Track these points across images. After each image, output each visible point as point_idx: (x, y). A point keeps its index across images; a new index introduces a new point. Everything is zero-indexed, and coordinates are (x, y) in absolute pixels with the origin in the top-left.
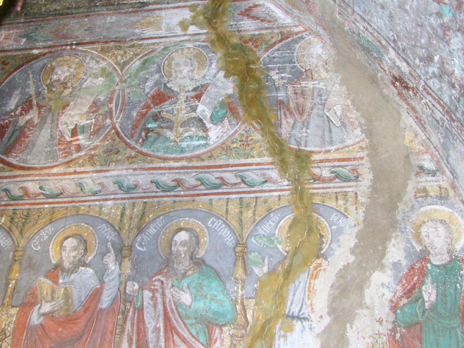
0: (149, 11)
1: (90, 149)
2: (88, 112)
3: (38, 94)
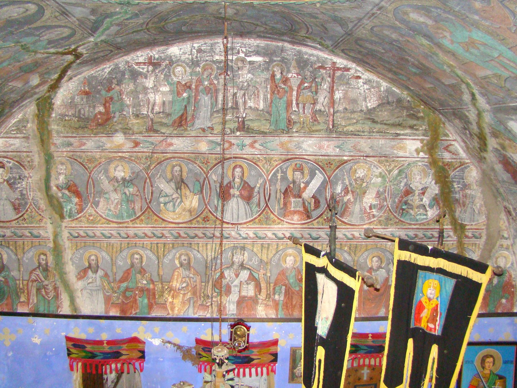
0: (400, 139)
2: (375, 197)
3: (351, 184)
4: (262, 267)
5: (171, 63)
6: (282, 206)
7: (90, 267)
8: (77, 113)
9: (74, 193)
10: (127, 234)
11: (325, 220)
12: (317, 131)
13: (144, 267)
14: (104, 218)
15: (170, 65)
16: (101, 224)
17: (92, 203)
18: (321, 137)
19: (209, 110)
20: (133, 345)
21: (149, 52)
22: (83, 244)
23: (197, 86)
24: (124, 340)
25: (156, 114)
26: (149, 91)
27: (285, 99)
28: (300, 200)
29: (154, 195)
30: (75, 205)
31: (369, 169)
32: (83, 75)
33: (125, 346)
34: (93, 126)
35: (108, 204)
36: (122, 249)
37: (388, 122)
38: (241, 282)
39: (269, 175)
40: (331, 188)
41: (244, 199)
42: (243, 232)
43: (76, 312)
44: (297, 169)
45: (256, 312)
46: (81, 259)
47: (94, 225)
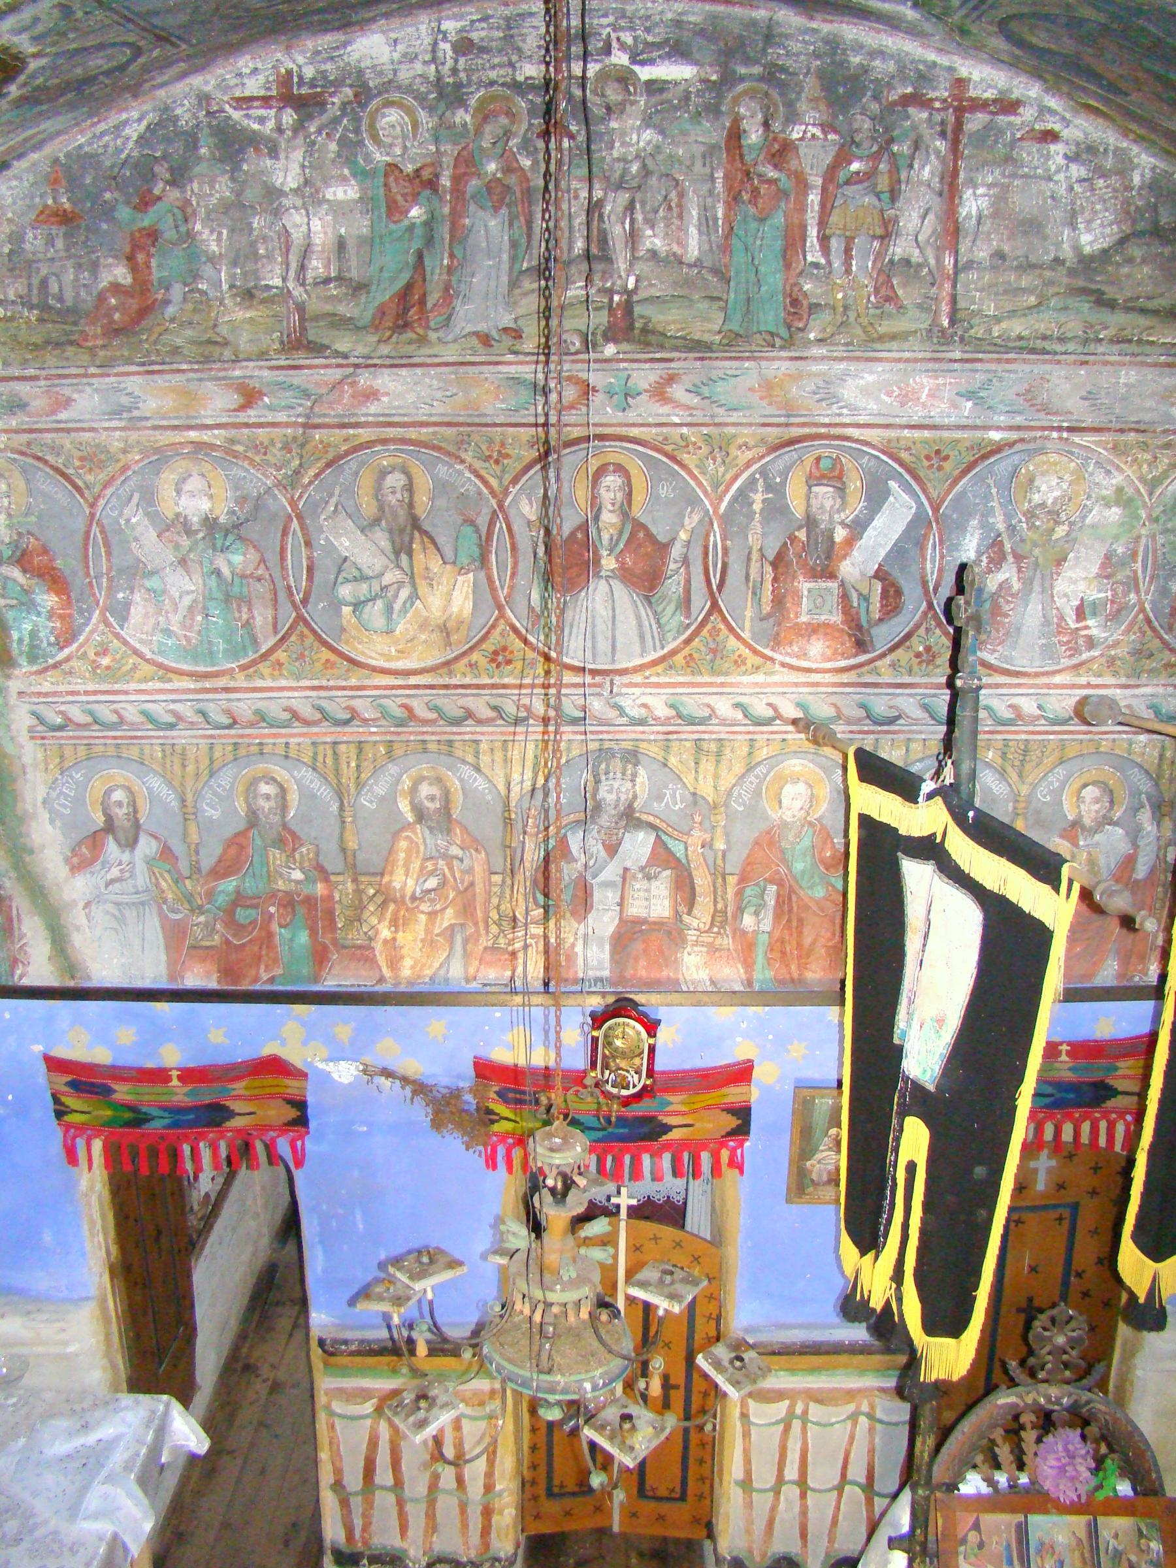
1: (1109, 647)
2: (1098, 576)
3: (1012, 529)
4: (698, 819)
5: (363, 95)
6: (767, 608)
7: (110, 826)
8: (35, 291)
9: (41, 576)
10: (228, 712)
11: (918, 655)
12: (893, 337)
13: (293, 826)
14: (147, 661)
15: (359, 103)
16: (140, 681)
17: (106, 609)
18: (907, 360)
19: (505, 266)
20: (269, 1081)
21: (279, 55)
22: (82, 752)
23: (457, 179)
24: (233, 1067)
25: (316, 284)
26: (286, 202)
27: (779, 219)
28: (833, 585)
29: (318, 577)
30: (50, 618)
31: (1079, 476)
32: (48, 150)
33: (239, 1087)
34: (95, 337)
35: (159, 613)
36: (216, 766)
37: (1154, 304)
38: (626, 870)
39: (721, 499)
40: (941, 542)
41: (633, 584)
42: (633, 699)
43: (73, 977)
44: (823, 476)
45: (676, 970)
46: (79, 801)
47: (117, 687)
